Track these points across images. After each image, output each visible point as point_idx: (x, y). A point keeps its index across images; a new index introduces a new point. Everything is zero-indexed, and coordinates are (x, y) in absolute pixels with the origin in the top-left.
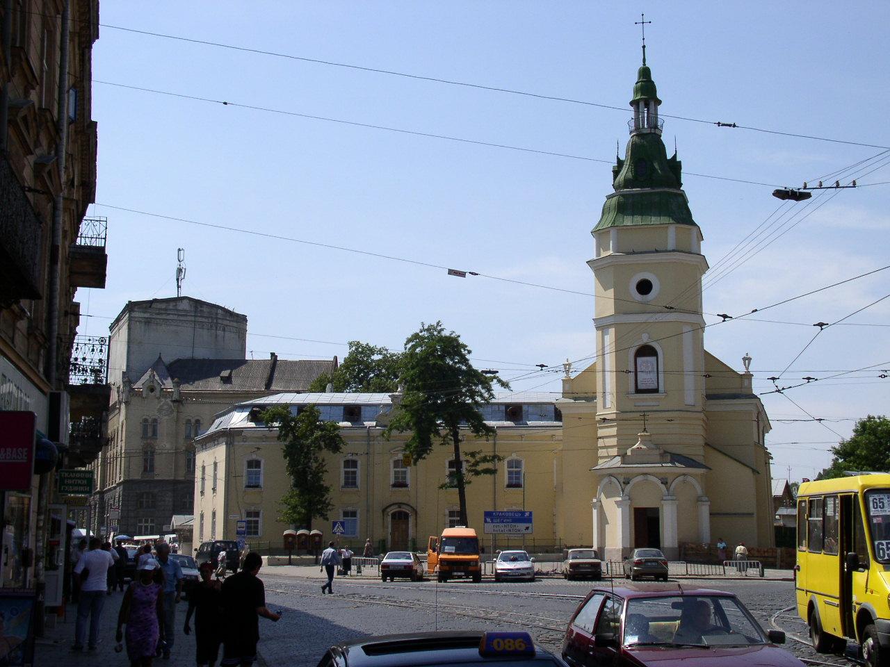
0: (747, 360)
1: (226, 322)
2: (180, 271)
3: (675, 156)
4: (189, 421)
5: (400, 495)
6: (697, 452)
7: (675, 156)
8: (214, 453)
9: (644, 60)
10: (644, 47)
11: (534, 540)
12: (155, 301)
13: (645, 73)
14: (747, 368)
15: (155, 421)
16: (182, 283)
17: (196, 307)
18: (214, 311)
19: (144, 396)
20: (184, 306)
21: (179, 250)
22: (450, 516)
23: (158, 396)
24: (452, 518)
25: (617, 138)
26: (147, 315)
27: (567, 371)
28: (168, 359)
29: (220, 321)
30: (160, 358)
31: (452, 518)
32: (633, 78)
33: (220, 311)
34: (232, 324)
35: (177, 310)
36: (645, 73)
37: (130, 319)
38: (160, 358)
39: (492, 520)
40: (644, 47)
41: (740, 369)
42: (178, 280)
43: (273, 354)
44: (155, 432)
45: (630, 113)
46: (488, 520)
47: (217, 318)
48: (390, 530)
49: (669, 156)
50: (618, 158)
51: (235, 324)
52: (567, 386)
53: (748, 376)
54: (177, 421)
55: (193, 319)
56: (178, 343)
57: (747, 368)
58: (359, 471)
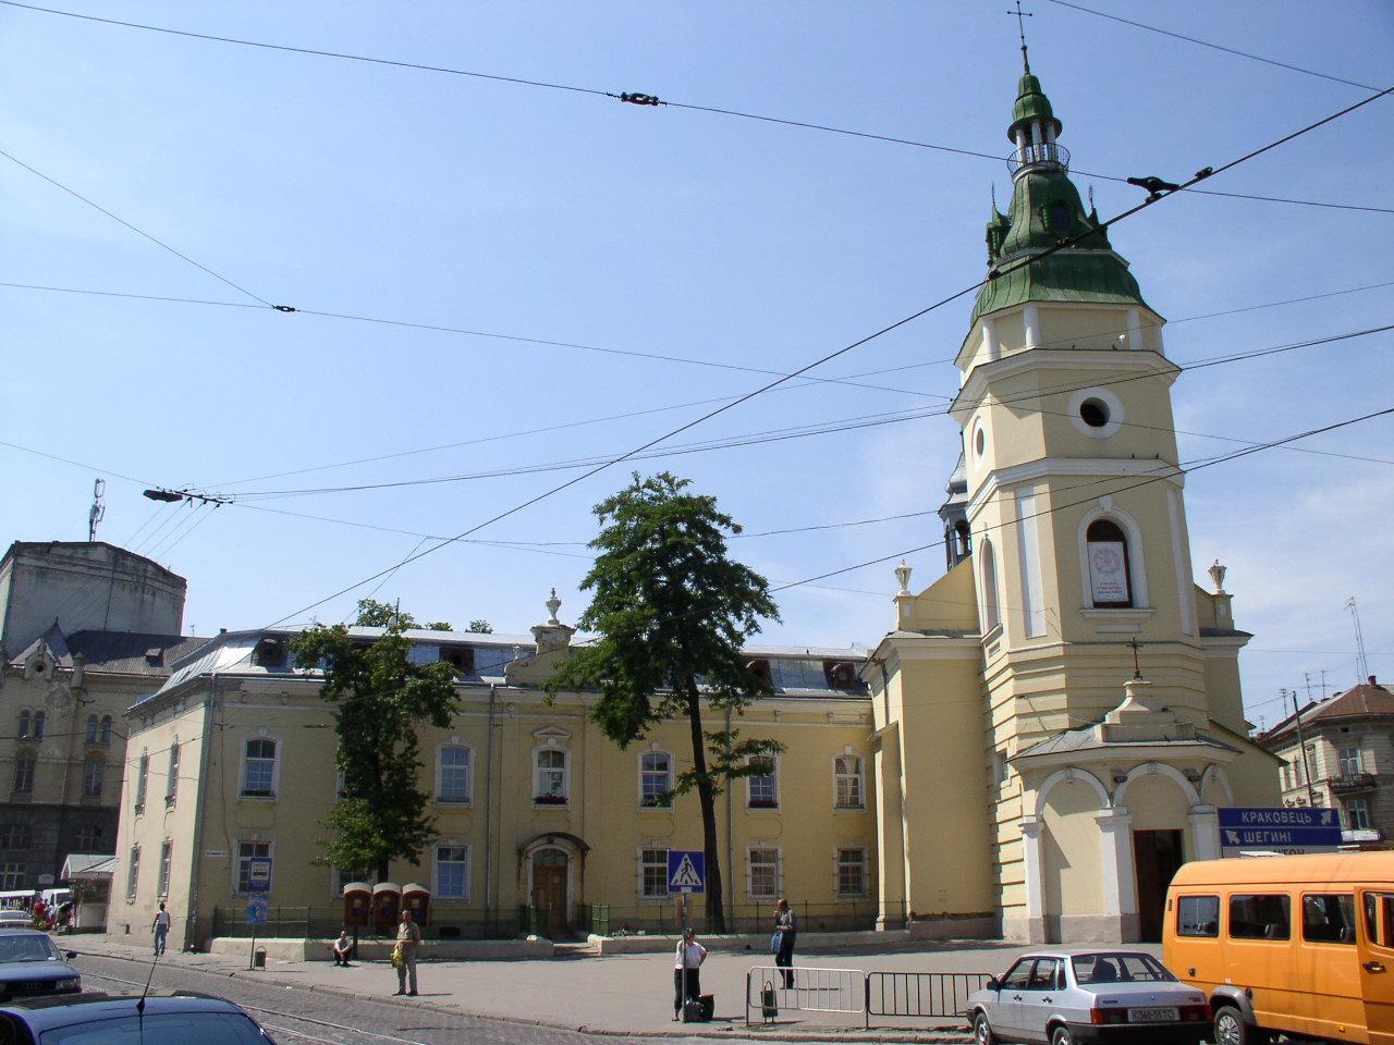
1: (157, 585)
2: (95, 510)
4: (93, 718)
5: (551, 820)
8: (173, 729)
9: (1027, 67)
10: (1024, 48)
11: (758, 905)
12: (56, 544)
13: (1032, 84)
15: (41, 714)
17: (116, 560)
18: (142, 566)
19: (27, 675)
21: (98, 481)
22: (645, 860)
23: (49, 677)
24: (756, 865)
25: (994, 183)
26: (42, 563)
27: (904, 582)
28: (68, 629)
29: (148, 581)
30: (56, 624)
31: (756, 865)
32: (1012, 89)
33: (150, 567)
37: (14, 567)
38: (56, 624)
39: (1240, 835)
40: (1024, 48)
42: (91, 522)
44: (38, 733)
46: (1232, 836)
47: (146, 577)
48: (530, 887)
49: (1088, 213)
51: (169, 589)
52: (907, 609)
53: (1224, 599)
54: (76, 717)
55: (109, 574)
56: (85, 607)
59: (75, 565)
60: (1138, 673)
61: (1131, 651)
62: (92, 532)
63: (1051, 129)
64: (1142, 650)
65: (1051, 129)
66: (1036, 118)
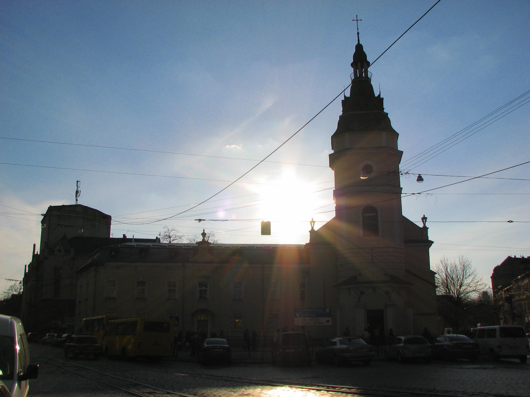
0: (424, 219)
2: (77, 192)
3: (380, 95)
7: (380, 95)
10: (358, 33)
13: (359, 48)
14: (424, 224)
16: (79, 199)
21: (77, 182)
32: (353, 51)
36: (359, 48)
40: (358, 33)
41: (421, 225)
42: (76, 197)
43: (124, 235)
45: (352, 70)
49: (376, 95)
50: (345, 96)
53: (425, 229)
57: (424, 224)
62: (77, 200)
66: (360, 60)
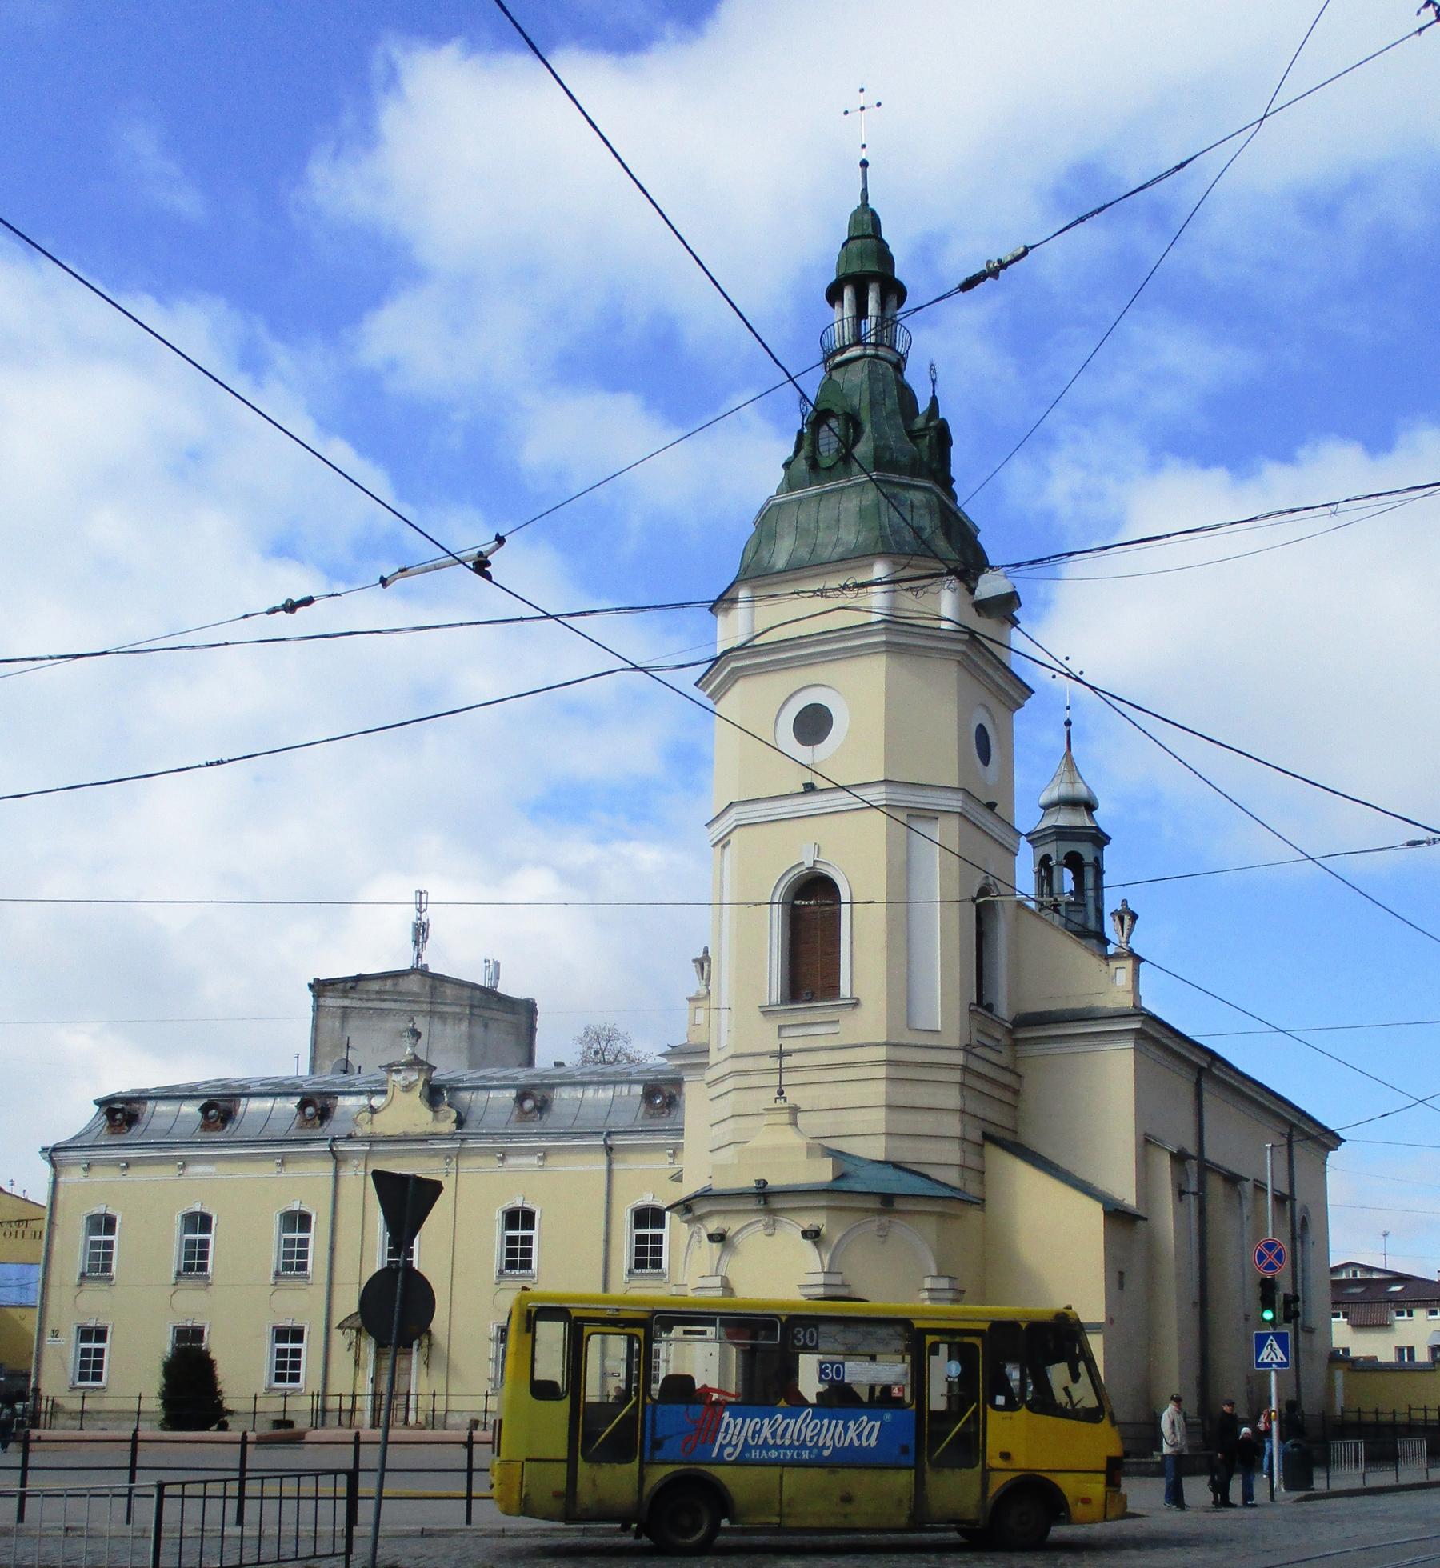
1: (487, 1014)
6: (943, 1158)
12: (360, 978)
17: (433, 988)
20: (413, 984)
26: (346, 1003)
34: (499, 1015)
35: (400, 993)
42: (417, 943)
48: (370, 1373)
55: (426, 1007)
58: (316, 1239)
59: (384, 1000)
60: (781, 1093)
61: (773, 1063)
63: (893, 301)
64: (787, 1062)
65: (893, 301)
